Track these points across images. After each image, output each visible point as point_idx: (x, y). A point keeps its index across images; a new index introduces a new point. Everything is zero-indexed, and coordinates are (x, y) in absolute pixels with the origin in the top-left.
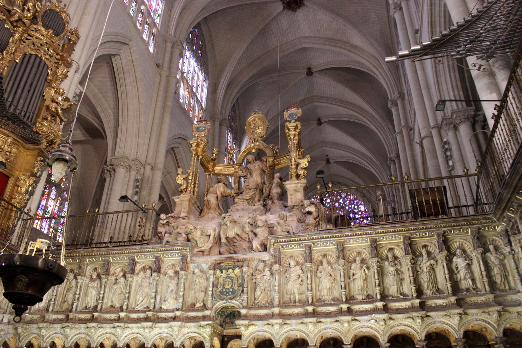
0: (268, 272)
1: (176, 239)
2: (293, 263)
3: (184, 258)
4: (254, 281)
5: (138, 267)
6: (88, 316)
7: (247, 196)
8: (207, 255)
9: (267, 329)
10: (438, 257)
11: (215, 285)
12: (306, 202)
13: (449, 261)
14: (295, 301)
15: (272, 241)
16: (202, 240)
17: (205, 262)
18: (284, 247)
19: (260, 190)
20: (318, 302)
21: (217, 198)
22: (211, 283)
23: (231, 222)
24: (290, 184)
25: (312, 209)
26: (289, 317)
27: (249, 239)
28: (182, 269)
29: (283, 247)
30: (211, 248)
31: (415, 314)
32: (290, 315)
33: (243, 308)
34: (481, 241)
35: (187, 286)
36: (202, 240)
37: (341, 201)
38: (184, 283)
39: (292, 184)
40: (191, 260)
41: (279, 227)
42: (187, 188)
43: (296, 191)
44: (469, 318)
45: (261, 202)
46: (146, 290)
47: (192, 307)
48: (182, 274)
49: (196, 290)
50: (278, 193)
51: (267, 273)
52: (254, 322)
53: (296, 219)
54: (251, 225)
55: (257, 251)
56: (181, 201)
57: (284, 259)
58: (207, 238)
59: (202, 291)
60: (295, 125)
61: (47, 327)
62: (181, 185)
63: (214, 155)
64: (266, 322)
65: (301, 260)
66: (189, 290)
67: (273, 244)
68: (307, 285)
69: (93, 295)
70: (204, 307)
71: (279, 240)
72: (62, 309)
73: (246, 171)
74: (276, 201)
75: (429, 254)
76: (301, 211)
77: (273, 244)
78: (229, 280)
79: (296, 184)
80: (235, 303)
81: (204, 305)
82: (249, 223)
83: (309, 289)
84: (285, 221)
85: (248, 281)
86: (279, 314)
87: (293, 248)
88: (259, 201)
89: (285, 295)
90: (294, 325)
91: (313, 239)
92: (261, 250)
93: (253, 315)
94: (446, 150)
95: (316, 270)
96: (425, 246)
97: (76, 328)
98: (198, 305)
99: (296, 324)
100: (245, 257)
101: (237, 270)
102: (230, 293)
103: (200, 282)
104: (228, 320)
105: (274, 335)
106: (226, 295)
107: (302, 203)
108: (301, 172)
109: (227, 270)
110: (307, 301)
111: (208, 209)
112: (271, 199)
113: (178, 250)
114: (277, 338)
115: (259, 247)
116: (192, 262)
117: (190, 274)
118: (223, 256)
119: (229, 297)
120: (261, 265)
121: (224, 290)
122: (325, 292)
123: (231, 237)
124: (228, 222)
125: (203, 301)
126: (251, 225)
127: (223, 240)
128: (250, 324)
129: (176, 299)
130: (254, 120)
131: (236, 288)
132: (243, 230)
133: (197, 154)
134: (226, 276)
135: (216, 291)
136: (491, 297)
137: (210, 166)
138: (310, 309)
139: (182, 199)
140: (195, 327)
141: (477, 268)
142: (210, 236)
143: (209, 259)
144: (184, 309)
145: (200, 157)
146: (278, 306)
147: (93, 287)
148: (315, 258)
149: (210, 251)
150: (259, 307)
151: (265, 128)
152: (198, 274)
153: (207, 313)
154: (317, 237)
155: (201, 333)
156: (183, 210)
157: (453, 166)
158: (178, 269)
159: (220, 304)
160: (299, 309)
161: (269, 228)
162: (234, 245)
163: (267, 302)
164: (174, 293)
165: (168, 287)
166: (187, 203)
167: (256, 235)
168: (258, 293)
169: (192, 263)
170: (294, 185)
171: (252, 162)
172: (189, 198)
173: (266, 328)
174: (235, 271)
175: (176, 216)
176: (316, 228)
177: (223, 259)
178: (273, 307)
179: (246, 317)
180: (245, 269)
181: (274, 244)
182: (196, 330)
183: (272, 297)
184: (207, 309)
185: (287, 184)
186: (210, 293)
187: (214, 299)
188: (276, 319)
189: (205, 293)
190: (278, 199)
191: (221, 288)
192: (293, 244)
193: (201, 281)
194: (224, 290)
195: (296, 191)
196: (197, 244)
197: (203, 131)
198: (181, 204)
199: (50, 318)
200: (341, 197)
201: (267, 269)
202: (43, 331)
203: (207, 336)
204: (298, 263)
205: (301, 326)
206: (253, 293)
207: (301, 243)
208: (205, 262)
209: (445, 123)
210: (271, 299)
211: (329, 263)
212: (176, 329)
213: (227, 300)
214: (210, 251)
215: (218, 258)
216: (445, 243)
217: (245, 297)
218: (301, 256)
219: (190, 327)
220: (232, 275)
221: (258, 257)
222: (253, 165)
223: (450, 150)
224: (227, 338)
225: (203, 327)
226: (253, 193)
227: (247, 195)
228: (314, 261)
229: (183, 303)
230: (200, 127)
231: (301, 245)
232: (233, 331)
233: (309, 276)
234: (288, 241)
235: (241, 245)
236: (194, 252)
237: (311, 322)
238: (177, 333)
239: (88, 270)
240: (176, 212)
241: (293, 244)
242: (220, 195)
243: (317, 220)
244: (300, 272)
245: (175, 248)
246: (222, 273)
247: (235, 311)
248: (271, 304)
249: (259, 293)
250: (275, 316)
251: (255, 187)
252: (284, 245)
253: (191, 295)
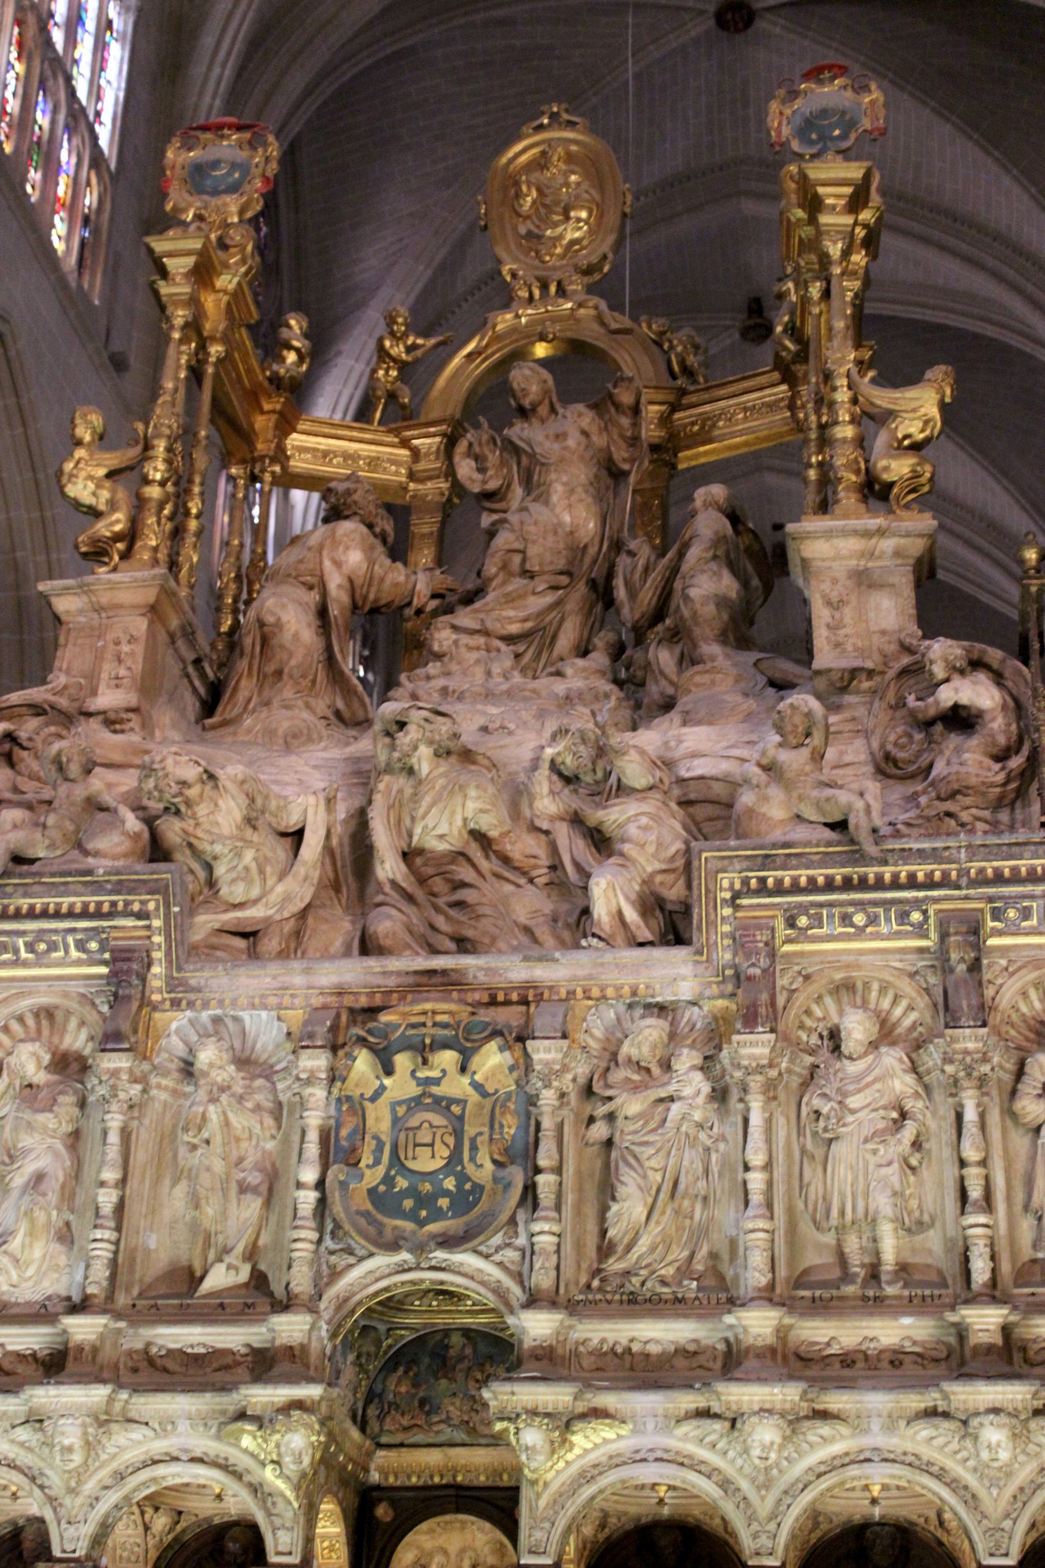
0: (698, 1076)
1: (79, 846)
2: (857, 1029)
3: (125, 967)
4: (599, 1131)
7: (512, 619)
8: (283, 955)
9: (691, 1448)
11: (337, 1150)
12: (942, 651)
14: (874, 1274)
15: (728, 880)
16: (249, 855)
17: (266, 1003)
18: (803, 921)
19: (593, 584)
21: (322, 612)
22: (313, 1136)
23: (442, 753)
24: (828, 534)
25: (979, 693)
26: (836, 1369)
27: (555, 867)
28: (111, 1039)
29: (791, 923)
30: (303, 915)
32: (847, 1360)
33: (533, 1301)
35: (140, 1156)
36: (249, 855)
38: (126, 1134)
39: (845, 533)
40: (173, 983)
41: (775, 792)
42: (131, 536)
43: (864, 580)
45: (599, 658)
47: (180, 1291)
48: (115, 1073)
49: (205, 1179)
50: (722, 602)
51: (691, 1084)
52: (608, 1400)
53: (863, 757)
54: (569, 780)
55: (620, 940)
56: (98, 609)
57: (800, 999)
58: (280, 851)
59: (243, 1189)
60: (855, 171)
62: (95, 514)
63: (291, 357)
64: (688, 1401)
65: (910, 1012)
66: (157, 1181)
67: (732, 903)
68: (951, 1172)
70: (262, 1294)
71: (771, 877)
73: (503, 463)
74: (711, 649)
76: (901, 703)
77: (732, 903)
78: (438, 1120)
79: (867, 534)
80: (475, 1270)
81: (259, 1281)
82: (555, 767)
83: (975, 1193)
84: (818, 757)
85: (560, 1128)
86: (772, 1351)
87: (860, 932)
89: (805, 1227)
90: (875, 1425)
91: (999, 879)
92: (645, 935)
93: (598, 1353)
95: (1008, 1078)
98: (219, 1278)
99: (891, 1422)
100: (541, 973)
101: (492, 1059)
102: (444, 1202)
103: (235, 1128)
104: (397, 1386)
105: (745, 1485)
106: (412, 1216)
107: (906, 660)
108: (897, 469)
109: (423, 1051)
110: (951, 1268)
111: (262, 679)
112: (675, 636)
113: (85, 914)
114: (764, 1506)
115: (631, 915)
116: (181, 995)
117: (166, 1074)
118: (394, 964)
119: (433, 1228)
120: (646, 1037)
121: (402, 1183)
123: (442, 847)
124: (425, 751)
125: (252, 1254)
126: (569, 780)
127: (388, 867)
128: (581, 1407)
129: (66, 1236)
130: (541, 163)
131: (483, 1170)
132: (515, 813)
133: (194, 327)
134: (413, 1090)
135: (343, 1185)
137: (263, 423)
138: (985, 1321)
139: (104, 599)
140: (202, 1420)
142: (297, 836)
143: (298, 980)
144: (122, 1300)
145: (216, 350)
146: (768, 1296)
148: (1004, 1001)
149: (298, 934)
150: (637, 1305)
151: (613, 219)
152: (220, 1076)
153: (290, 1328)
154: (1023, 865)
155: (243, 1462)
156: (108, 669)
158: (77, 1039)
159: (370, 1274)
160: (907, 1321)
161: (685, 803)
162: (460, 904)
163: (685, 1270)
164: (53, 1198)
166: (140, 625)
167: (601, 842)
168: (630, 1207)
169: (176, 1004)
170: (853, 544)
171: (543, 410)
172: (150, 595)
173: (686, 1439)
174: (476, 1061)
175: (63, 702)
176: (1004, 816)
177: (392, 982)
178: (733, 1303)
179: (551, 1362)
180: (544, 1052)
181: (736, 895)
182: (205, 1444)
183: (718, 1241)
184: (285, 1305)
185: (807, 536)
186: (308, 1198)
187: (328, 1243)
188: (761, 1380)
189: (268, 1203)
190: (723, 638)
191: (381, 1170)
192: (860, 905)
193: (239, 1121)
194: (402, 1183)
195: (864, 580)
196: (211, 883)
197: (234, 189)
198: (99, 632)
201: (687, 1059)
203: (281, 1485)
204: (886, 1033)
205: (924, 1431)
206: (591, 1211)
207: (917, 903)
208: (266, 1003)
210: (713, 1256)
212: (70, 1434)
213: (419, 1249)
214: (298, 934)
215: (355, 973)
217: (544, 1232)
218: (907, 987)
219: (167, 1425)
220: (457, 1086)
221: (627, 980)
222: (554, 426)
224: (393, 1503)
225: (258, 1420)
226: (550, 598)
227: (511, 608)
228: (995, 1019)
229: (114, 1264)
230: (215, 164)
231: (916, 916)
232: (433, 1458)
233: (970, 1115)
234: (830, 886)
235: (505, 900)
236: (197, 936)
237: (996, 1411)
238: (77, 1458)
240: (59, 679)
241: (860, 905)
242: (345, 598)
243: (1016, 762)
244: (903, 1084)
245: (66, 901)
246: (389, 1071)
247: (447, 1332)
248: (710, 1282)
249: (639, 1212)
250: (750, 1363)
251: (561, 564)
252: (803, 909)
253: (167, 1214)
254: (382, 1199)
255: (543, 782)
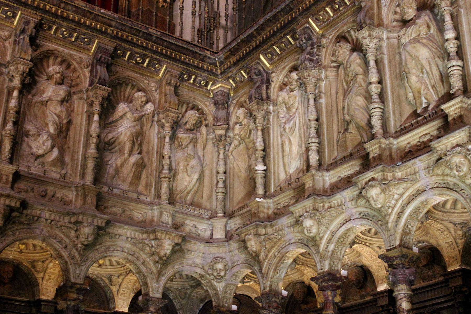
61: (315, 210)
69: (424, 62)
72: (346, 147)
97: (401, 180)
147: (416, 40)
199: (319, 185)
202: (308, 223)
239: (384, 11)
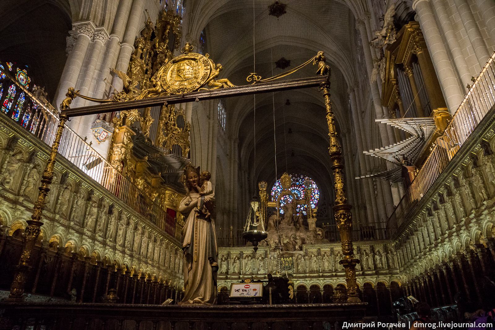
2: (313, 256)
5: (244, 255)
6: (224, 277)
10: (370, 255)
12: (318, 229)
13: (374, 257)
20: (324, 271)
25: (320, 233)
31: (360, 277)
32: (313, 276)
33: (294, 274)
34: (386, 250)
37: (300, 181)
44: (380, 278)
46: (250, 265)
75: (366, 253)
88: (292, 222)
94: (374, 185)
96: (365, 250)
101: (290, 258)
108: (314, 215)
122: (326, 268)
127: (282, 245)
136: (388, 271)
141: (384, 259)
147: (224, 264)
157: (377, 194)
165: (260, 264)
168: (299, 267)
180: (294, 258)
200: (301, 178)
209: (374, 170)
211: (327, 256)
216: (373, 250)
220: (288, 260)
223: (376, 185)
227: (286, 220)
244: (316, 259)
254: (284, 267)
255: (292, 238)
